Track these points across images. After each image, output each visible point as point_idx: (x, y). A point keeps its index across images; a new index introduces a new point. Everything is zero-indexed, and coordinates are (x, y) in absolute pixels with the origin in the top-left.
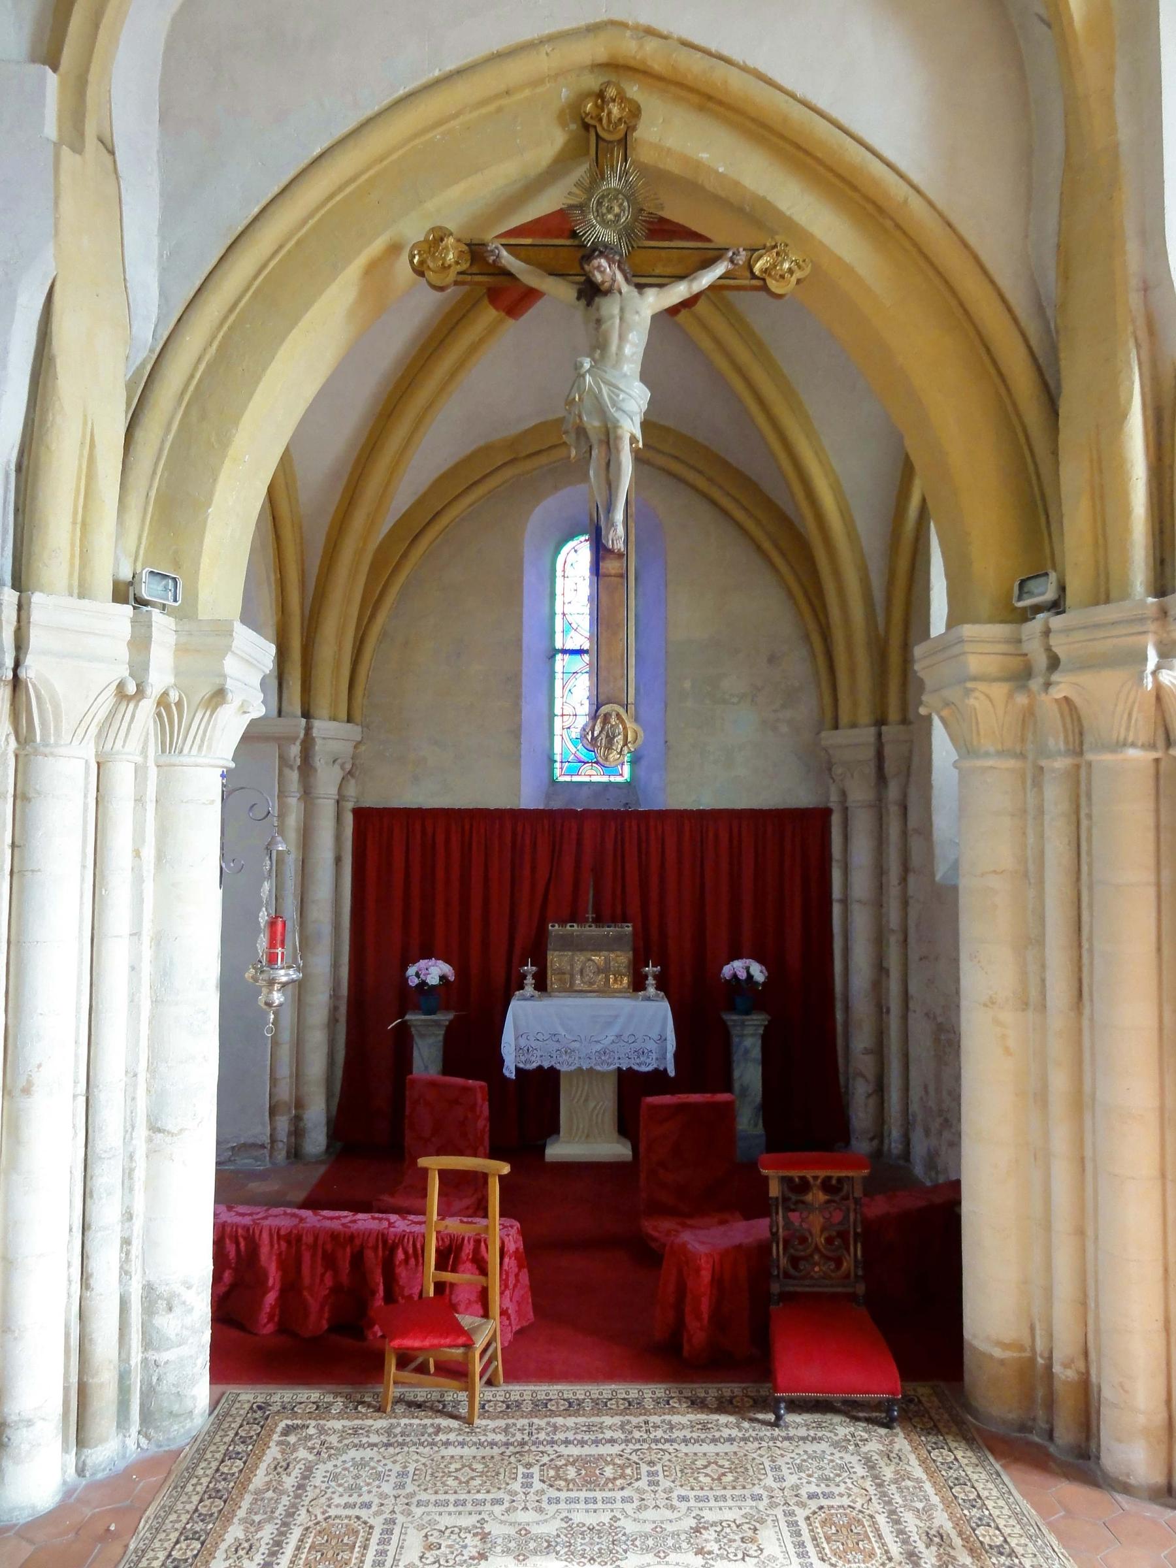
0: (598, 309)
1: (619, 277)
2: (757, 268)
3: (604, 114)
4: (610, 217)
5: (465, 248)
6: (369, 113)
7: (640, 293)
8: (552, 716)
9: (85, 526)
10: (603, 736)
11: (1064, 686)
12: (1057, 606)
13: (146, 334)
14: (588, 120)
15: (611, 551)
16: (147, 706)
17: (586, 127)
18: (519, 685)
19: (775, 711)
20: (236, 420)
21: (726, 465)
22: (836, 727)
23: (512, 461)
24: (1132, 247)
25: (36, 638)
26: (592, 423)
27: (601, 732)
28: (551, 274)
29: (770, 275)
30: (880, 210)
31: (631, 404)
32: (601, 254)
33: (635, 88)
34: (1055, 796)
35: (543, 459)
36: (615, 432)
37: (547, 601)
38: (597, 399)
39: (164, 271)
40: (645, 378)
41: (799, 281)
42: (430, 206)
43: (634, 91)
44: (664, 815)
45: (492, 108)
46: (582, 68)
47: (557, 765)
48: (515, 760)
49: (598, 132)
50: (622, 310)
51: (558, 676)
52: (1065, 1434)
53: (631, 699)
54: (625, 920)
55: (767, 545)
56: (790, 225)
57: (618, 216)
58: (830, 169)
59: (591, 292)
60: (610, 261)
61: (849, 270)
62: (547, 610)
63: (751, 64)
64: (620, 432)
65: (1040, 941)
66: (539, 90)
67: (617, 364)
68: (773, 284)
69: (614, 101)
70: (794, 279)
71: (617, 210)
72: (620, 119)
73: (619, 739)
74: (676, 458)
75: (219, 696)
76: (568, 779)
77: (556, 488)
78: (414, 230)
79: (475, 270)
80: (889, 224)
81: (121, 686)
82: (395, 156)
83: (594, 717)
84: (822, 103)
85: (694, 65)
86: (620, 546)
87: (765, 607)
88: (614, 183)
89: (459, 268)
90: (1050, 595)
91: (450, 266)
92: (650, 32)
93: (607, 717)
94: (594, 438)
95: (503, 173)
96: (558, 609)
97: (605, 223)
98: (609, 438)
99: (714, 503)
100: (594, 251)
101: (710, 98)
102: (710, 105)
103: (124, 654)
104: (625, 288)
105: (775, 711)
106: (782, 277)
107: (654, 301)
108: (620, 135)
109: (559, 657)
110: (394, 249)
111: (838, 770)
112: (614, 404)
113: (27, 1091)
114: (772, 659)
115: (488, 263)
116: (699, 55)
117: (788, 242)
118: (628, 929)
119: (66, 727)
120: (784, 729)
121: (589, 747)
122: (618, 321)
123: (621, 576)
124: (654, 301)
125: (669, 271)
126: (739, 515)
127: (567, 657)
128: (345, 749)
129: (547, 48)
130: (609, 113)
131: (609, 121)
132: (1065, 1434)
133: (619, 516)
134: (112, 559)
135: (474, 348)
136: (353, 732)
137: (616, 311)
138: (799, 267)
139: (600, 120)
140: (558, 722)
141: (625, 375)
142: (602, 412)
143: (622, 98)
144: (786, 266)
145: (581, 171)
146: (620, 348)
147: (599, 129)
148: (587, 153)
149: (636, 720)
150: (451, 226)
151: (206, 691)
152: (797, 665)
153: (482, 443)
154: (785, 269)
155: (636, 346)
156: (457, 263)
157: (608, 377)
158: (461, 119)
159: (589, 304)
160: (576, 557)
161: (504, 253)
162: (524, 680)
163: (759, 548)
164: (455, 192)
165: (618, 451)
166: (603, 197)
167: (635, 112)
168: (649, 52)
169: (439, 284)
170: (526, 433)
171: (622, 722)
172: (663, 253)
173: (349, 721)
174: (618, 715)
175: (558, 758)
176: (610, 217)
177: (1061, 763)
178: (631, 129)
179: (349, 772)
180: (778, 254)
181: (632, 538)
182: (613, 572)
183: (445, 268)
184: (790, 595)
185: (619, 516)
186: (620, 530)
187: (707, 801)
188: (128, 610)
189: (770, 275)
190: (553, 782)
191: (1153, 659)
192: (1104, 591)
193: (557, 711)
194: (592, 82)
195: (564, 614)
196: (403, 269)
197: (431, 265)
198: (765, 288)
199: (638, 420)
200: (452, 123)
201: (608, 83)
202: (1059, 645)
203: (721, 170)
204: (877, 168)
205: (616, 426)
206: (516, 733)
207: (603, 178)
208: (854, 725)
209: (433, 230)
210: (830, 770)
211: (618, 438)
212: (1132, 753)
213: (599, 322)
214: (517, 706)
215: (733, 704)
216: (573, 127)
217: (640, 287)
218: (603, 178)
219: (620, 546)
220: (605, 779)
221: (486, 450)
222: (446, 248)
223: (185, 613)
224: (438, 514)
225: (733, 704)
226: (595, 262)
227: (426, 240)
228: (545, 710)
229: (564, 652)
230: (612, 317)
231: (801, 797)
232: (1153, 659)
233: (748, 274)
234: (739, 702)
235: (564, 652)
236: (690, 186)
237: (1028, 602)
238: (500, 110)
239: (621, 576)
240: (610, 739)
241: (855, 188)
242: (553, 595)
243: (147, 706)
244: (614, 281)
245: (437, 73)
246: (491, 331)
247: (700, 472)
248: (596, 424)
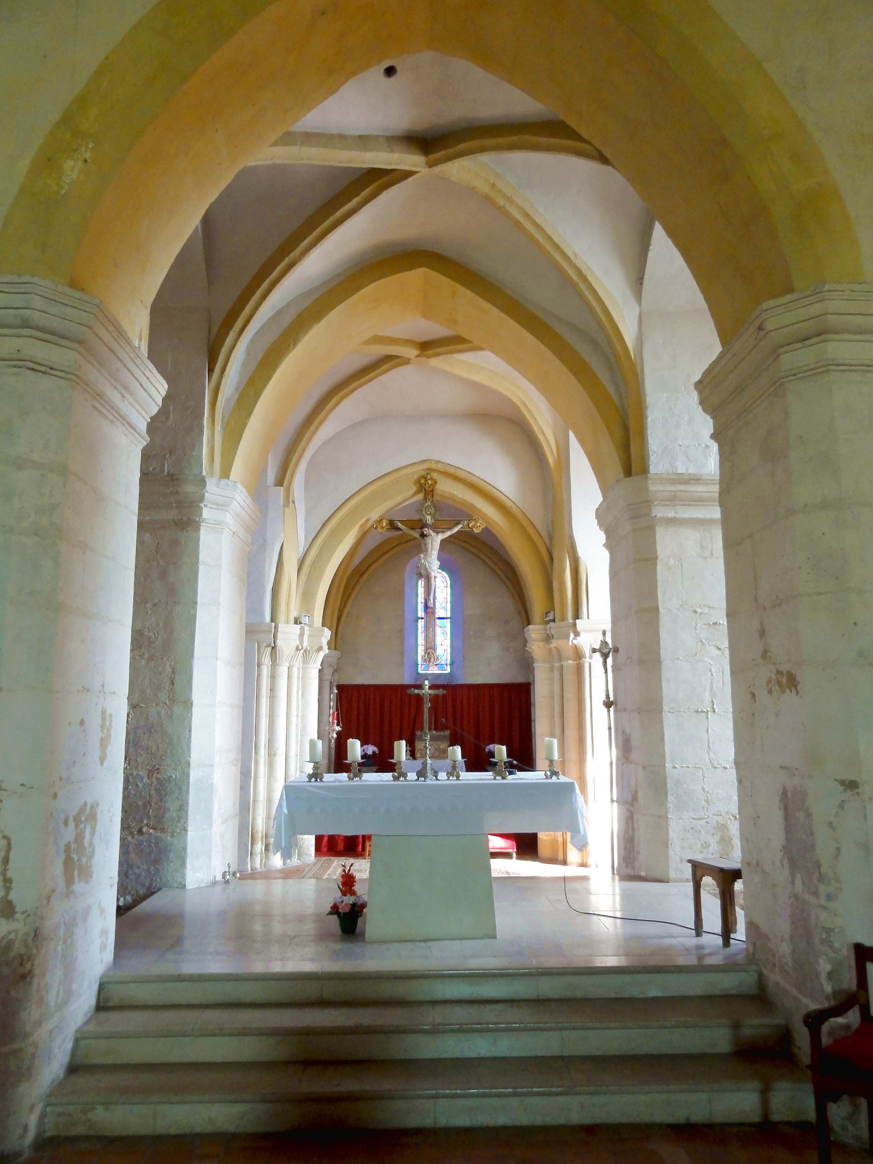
8: (417, 646)
9: (288, 604)
11: (554, 644)
12: (554, 620)
13: (301, 550)
16: (302, 651)
20: (324, 571)
24: (566, 526)
25: (279, 635)
34: (556, 674)
38: (425, 566)
39: (307, 531)
40: (439, 559)
43: (435, 475)
44: (462, 686)
49: (425, 487)
52: (561, 857)
54: (447, 729)
55: (503, 577)
59: (423, 536)
61: (497, 524)
65: (554, 716)
74: (466, 542)
75: (320, 648)
78: (374, 515)
81: (297, 647)
85: (451, 470)
86: (432, 606)
87: (503, 600)
90: (551, 617)
92: (439, 462)
103: (296, 637)
107: (441, 537)
110: (368, 520)
113: (275, 755)
114: (506, 622)
118: (447, 733)
119: (284, 658)
124: (441, 537)
128: (335, 661)
132: (561, 857)
134: (294, 614)
136: (337, 654)
142: (426, 569)
143: (432, 479)
151: (316, 648)
163: (499, 577)
167: (436, 482)
168: (439, 467)
173: (335, 649)
177: (557, 665)
179: (336, 671)
183: (383, 528)
184: (513, 597)
187: (479, 680)
188: (299, 626)
190: (418, 673)
191: (572, 636)
192: (563, 619)
194: (424, 473)
202: (553, 632)
204: (503, 498)
206: (402, 653)
212: (570, 662)
214: (402, 643)
217: (437, 533)
220: (440, 672)
223: (311, 625)
224: (370, 565)
231: (519, 679)
232: (572, 636)
237: (548, 619)
243: (302, 651)
247: (475, 547)
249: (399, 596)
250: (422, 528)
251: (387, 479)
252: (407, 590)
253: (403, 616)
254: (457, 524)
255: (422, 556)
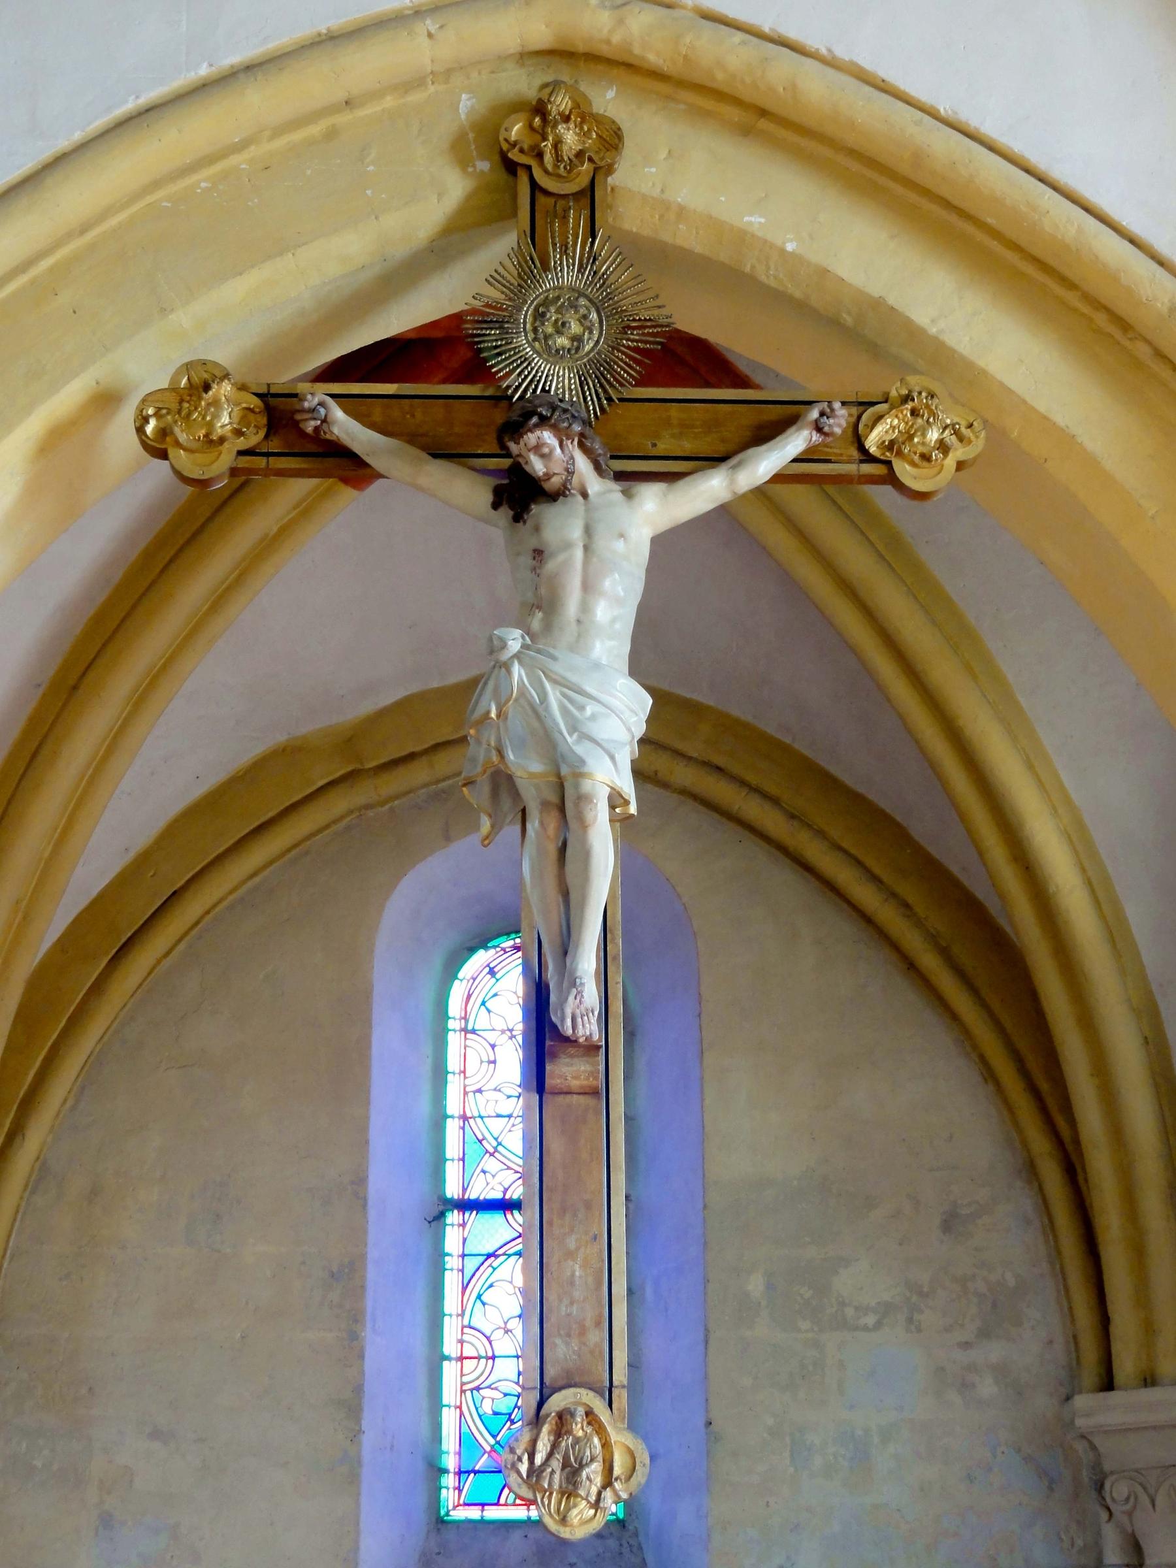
0: (537, 529)
1: (583, 464)
2: (872, 443)
3: (547, 146)
4: (562, 341)
5: (255, 402)
6: (63, 144)
7: (628, 494)
8: (437, 1359)
10: (556, 1464)
14: (514, 155)
15: (567, 1040)
17: (511, 167)
18: (358, 1291)
19: (966, 1345)
21: (829, 784)
22: (1108, 1384)
23: (350, 777)
26: (527, 766)
27: (550, 1455)
28: (435, 456)
29: (899, 454)
30: (1124, 325)
31: (607, 721)
32: (544, 421)
33: (611, 94)
35: (418, 774)
36: (577, 786)
37: (426, 1088)
38: (537, 713)
40: (636, 670)
41: (960, 466)
42: (183, 318)
43: (607, 100)
45: (315, 130)
46: (502, 58)
47: (449, 1480)
48: (348, 1471)
49: (534, 176)
50: (588, 531)
51: (452, 1262)
53: (620, 1376)
55: (929, 961)
56: (940, 357)
57: (577, 339)
58: (1015, 247)
59: (521, 494)
60: (562, 435)
61: (1065, 440)
62: (424, 1106)
63: (842, 53)
64: (586, 785)
66: (415, 97)
67: (579, 645)
68: (903, 470)
69: (567, 119)
70: (950, 462)
71: (575, 328)
72: (580, 154)
73: (593, 1472)
76: (474, 1514)
77: (448, 838)
78: (149, 368)
79: (274, 445)
80: (1142, 351)
82: (114, 221)
83: (537, 1421)
84: (989, 128)
86: (590, 1029)
87: (926, 1098)
88: (569, 277)
89: (242, 443)
91: (222, 440)
93: (564, 1418)
94: (531, 797)
95: (339, 254)
96: (453, 1105)
97: (556, 355)
98: (563, 799)
99: (807, 868)
100: (528, 415)
101: (763, 113)
102: (763, 124)
104: (596, 485)
105: (966, 1345)
106: (926, 458)
108: (583, 181)
109: (453, 1217)
110: (105, 401)
111: (1118, 1490)
112: (574, 728)
114: (951, 1223)
115: (303, 434)
116: (739, 37)
117: (936, 387)
120: (987, 1387)
121: (526, 1493)
122: (579, 553)
123: (595, 1093)
124: (655, 510)
125: (687, 446)
126: (866, 895)
127: (472, 1217)
129: (431, 24)
130: (557, 144)
131: (558, 158)
133: (587, 962)
135: (268, 547)
137: (576, 533)
138: (961, 439)
139: (540, 156)
140: (450, 1371)
141: (597, 666)
143: (582, 115)
144: (933, 435)
145: (501, 248)
146: (585, 608)
147: (537, 173)
148: (514, 213)
149: (632, 1427)
150: (223, 355)
152: (1010, 1241)
153: (280, 738)
154: (933, 450)
155: (619, 602)
156: (238, 433)
157: (558, 668)
158: (253, 151)
159: (518, 518)
160: (491, 996)
161: (338, 414)
162: (372, 1273)
163: (910, 966)
164: (236, 290)
165: (584, 827)
166: (546, 303)
167: (612, 139)
169: (196, 474)
170: (382, 714)
171: (600, 1430)
172: (674, 410)
174: (589, 1413)
175: (450, 1462)
176: (562, 341)
178: (602, 170)
180: (914, 413)
181: (617, 1007)
182: (575, 1084)
183: (212, 443)
184: (989, 1074)
185: (587, 962)
186: (591, 994)
189: (899, 454)
190: (440, 1523)
193: (450, 1347)
194: (523, 84)
195: (464, 1118)
196: (120, 438)
197: (182, 437)
198: (891, 479)
199: (626, 756)
200: (234, 160)
201: (554, 86)
203: (790, 247)
205: (579, 775)
206: (351, 1406)
207: (546, 268)
208: (1149, 1380)
209: (188, 367)
210: (1100, 1487)
211: (583, 799)
213: (539, 554)
215: (866, 1328)
216: (484, 166)
218: (546, 268)
219: (590, 1029)
221: (289, 754)
222: (216, 403)
225: (866, 1328)
226: (531, 438)
227: (173, 389)
228: (420, 1349)
229: (466, 1205)
230: (568, 546)
233: (855, 453)
234: (878, 1325)
235: (466, 1205)
236: (727, 272)
238: (331, 134)
239: (595, 1093)
240: (572, 1471)
241: (1071, 285)
242: (440, 1074)
244: (570, 473)
245: (204, 71)
246: (305, 511)
247: (775, 801)
248: (536, 766)
249: (337, 1066)
250: (514, 428)
251: (257, 104)
252: (387, 1036)
253: (356, 1185)
254: (766, 433)
255: (514, 640)
